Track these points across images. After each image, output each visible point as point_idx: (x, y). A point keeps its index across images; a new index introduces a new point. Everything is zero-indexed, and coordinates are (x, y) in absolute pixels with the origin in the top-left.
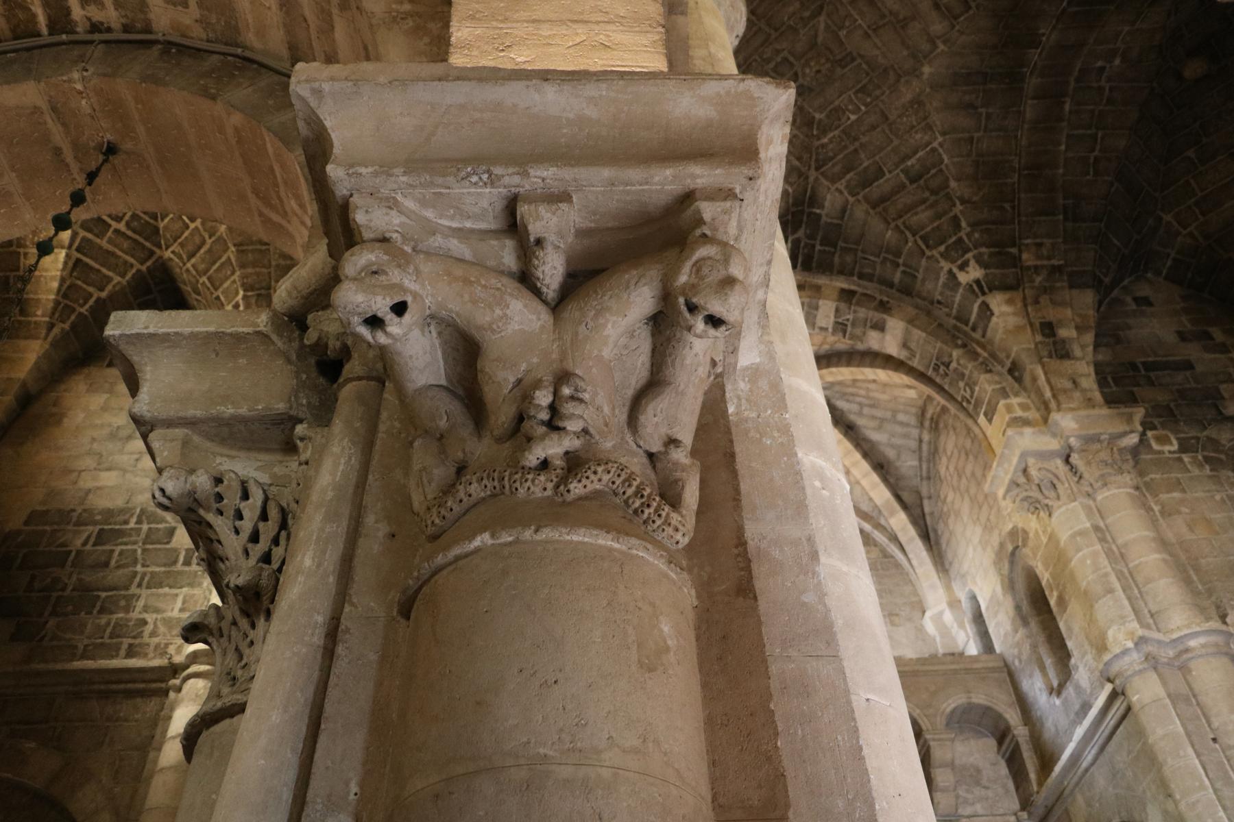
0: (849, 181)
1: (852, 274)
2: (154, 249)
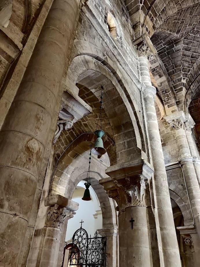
1: (164, 63)
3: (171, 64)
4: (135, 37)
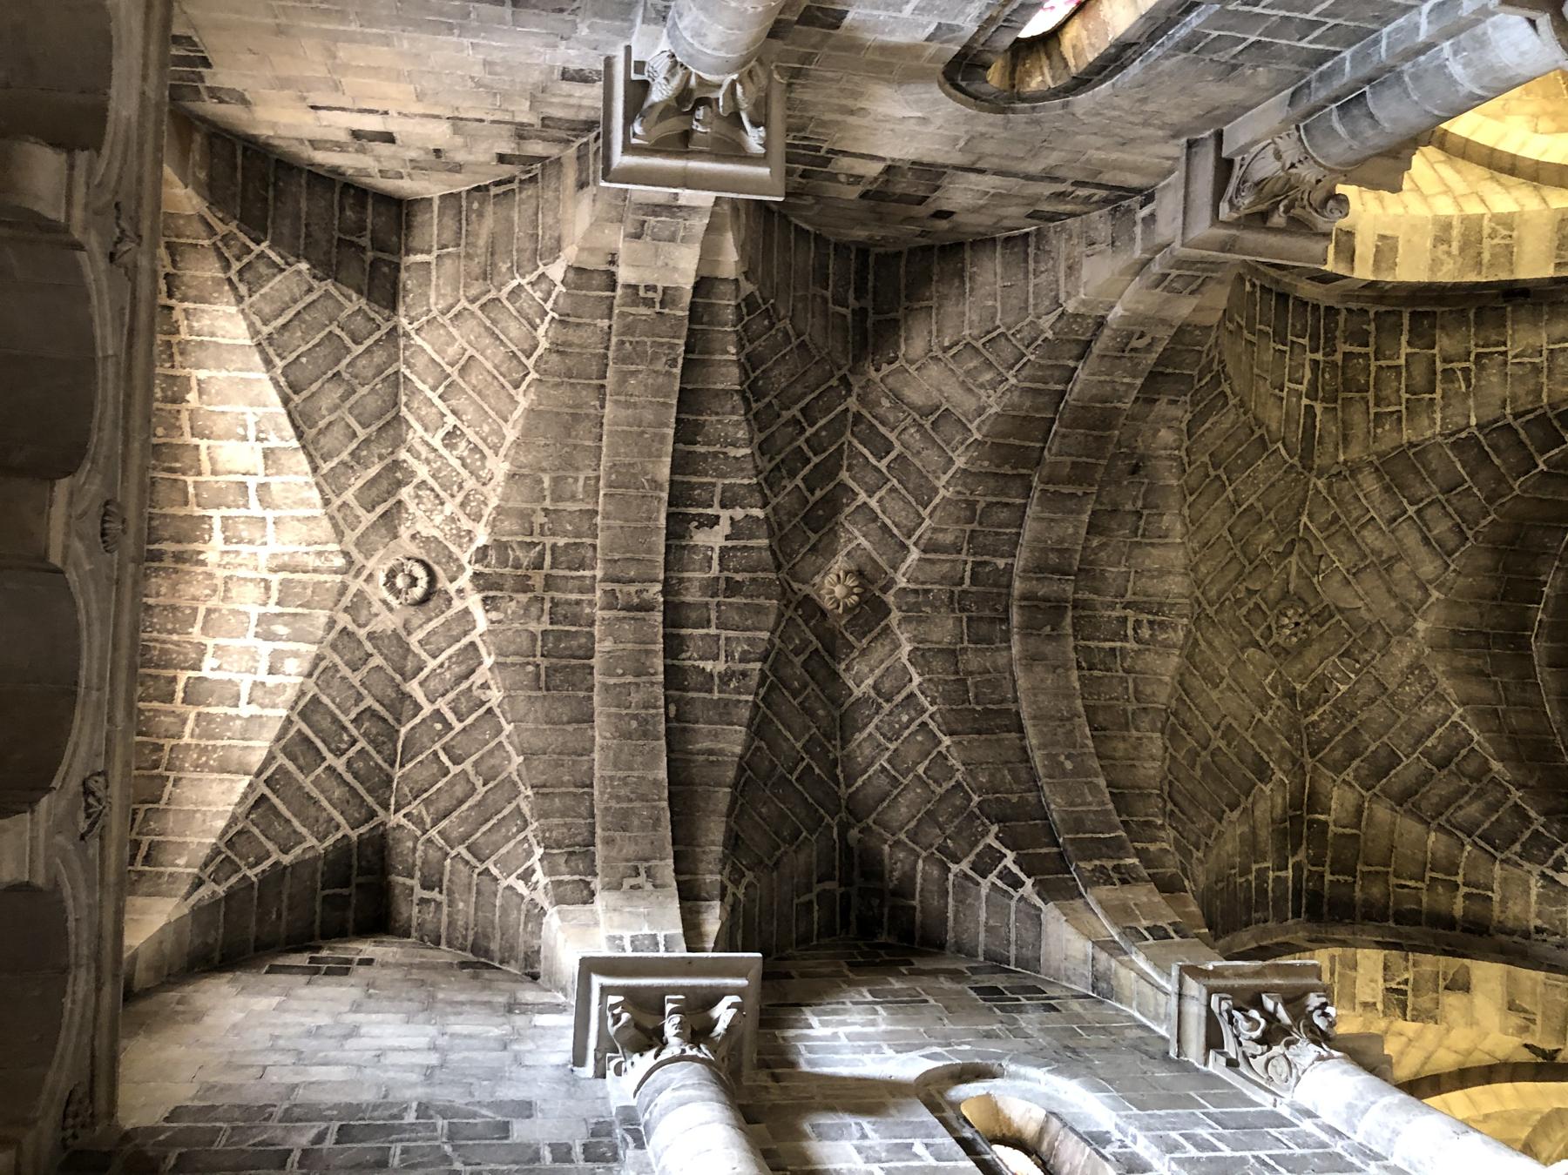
0: (1356, 770)
2: (377, 808)
3: (1419, 884)
4: (1156, 1018)
